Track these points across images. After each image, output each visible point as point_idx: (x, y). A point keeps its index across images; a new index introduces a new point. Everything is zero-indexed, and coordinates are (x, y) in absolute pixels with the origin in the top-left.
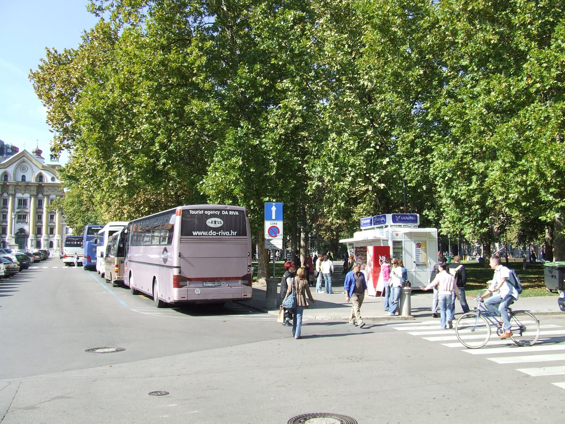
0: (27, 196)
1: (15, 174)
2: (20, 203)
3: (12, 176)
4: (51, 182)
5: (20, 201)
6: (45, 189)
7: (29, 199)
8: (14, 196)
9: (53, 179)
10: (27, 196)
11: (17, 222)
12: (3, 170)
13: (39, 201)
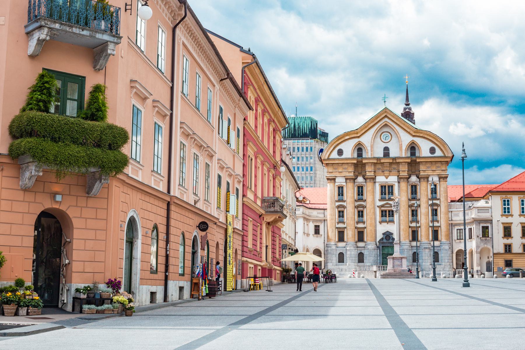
0: (393, 179)
1: (372, 147)
2: (383, 193)
3: (369, 148)
4: (430, 155)
5: (383, 187)
6: (422, 168)
7: (396, 184)
8: (373, 179)
9: (432, 150)
10: (393, 179)
11: (381, 223)
12: (356, 141)
13: (412, 186)
